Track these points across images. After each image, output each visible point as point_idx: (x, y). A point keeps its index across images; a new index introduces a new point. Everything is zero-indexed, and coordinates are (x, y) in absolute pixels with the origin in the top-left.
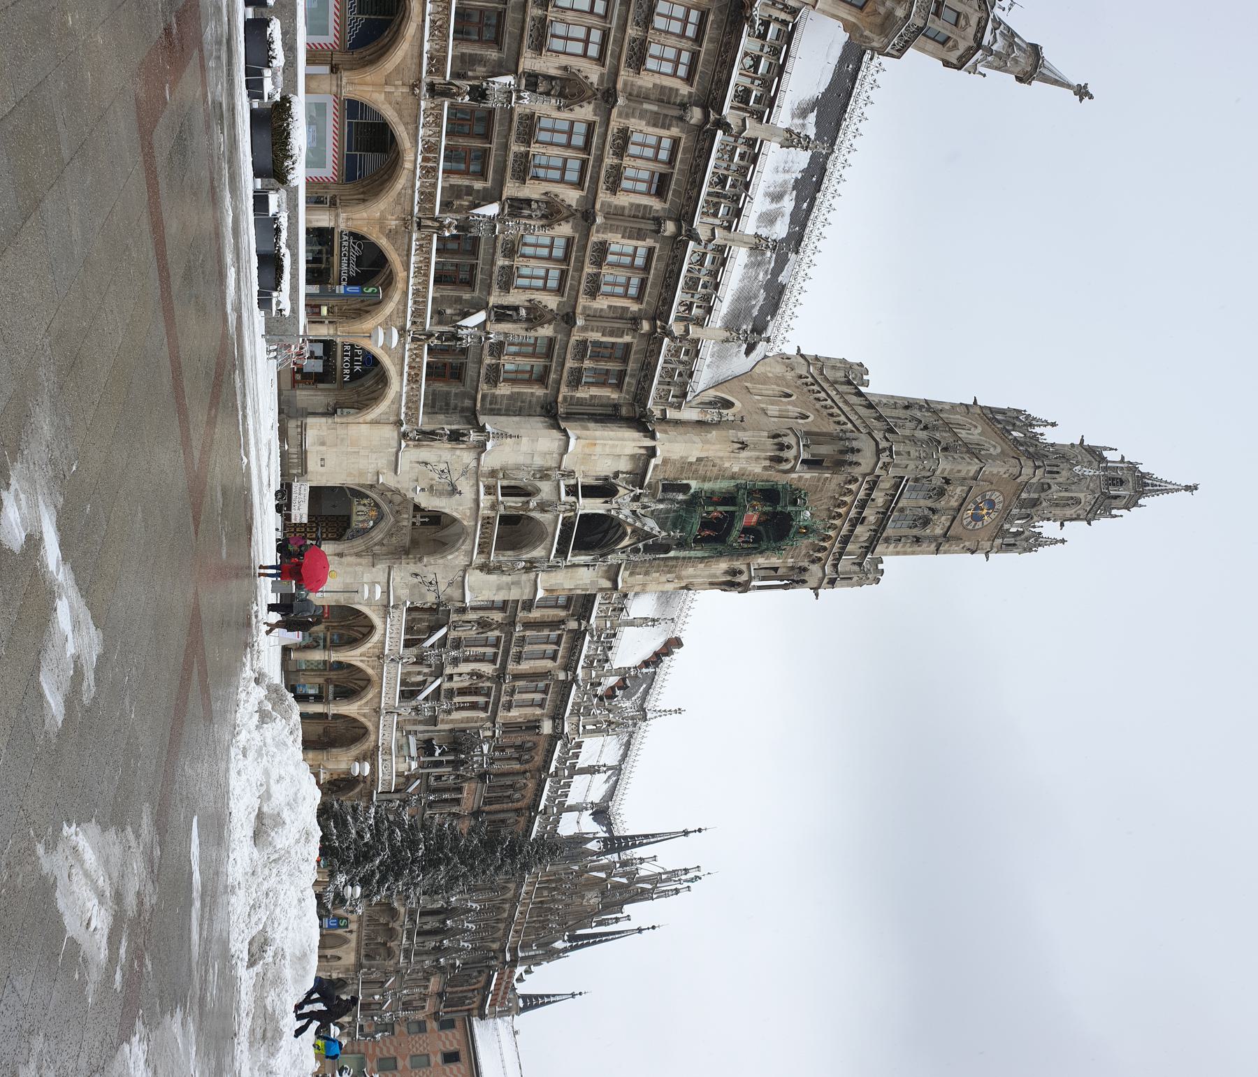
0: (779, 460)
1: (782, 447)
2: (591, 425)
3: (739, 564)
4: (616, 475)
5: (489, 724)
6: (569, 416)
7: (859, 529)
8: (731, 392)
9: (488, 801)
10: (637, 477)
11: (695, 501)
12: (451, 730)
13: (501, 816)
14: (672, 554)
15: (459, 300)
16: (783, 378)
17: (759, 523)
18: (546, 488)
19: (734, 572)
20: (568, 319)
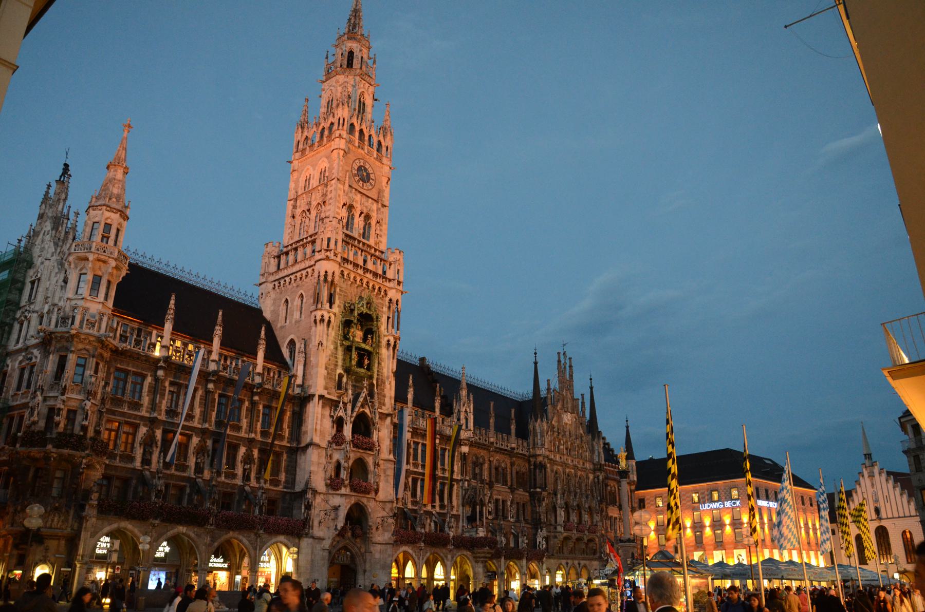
0: (329, 322)
1: (322, 320)
2: (303, 429)
3: (384, 342)
4: (332, 417)
5: (461, 484)
6: (299, 442)
7: (370, 266)
8: (284, 338)
9: (505, 483)
10: (334, 404)
11: (348, 370)
12: (463, 506)
13: (514, 472)
14: (375, 382)
15: (239, 502)
16: (275, 300)
17: (361, 330)
18: (337, 456)
19: (388, 344)
20: (251, 442)
